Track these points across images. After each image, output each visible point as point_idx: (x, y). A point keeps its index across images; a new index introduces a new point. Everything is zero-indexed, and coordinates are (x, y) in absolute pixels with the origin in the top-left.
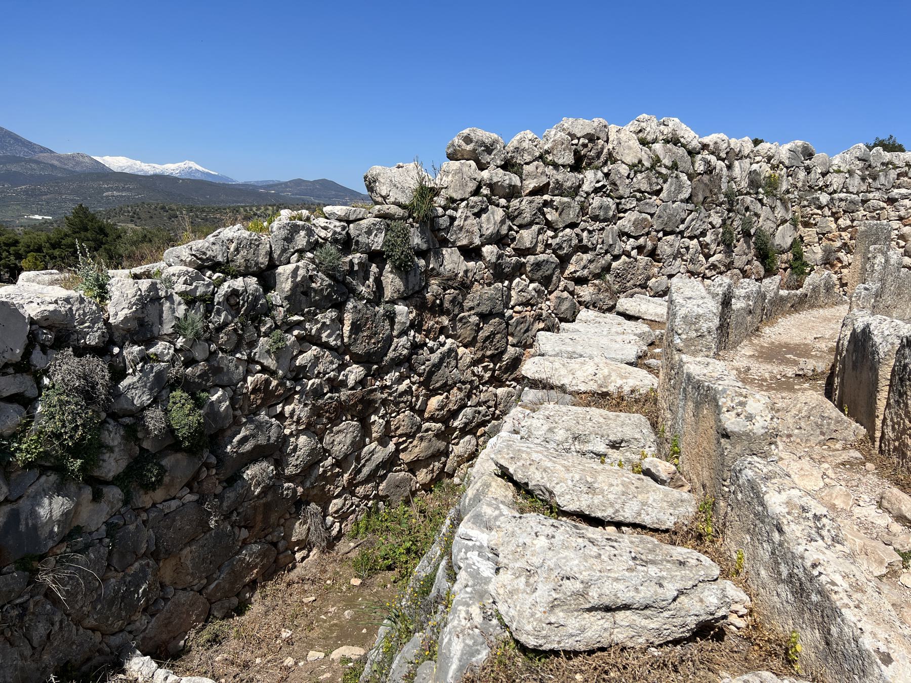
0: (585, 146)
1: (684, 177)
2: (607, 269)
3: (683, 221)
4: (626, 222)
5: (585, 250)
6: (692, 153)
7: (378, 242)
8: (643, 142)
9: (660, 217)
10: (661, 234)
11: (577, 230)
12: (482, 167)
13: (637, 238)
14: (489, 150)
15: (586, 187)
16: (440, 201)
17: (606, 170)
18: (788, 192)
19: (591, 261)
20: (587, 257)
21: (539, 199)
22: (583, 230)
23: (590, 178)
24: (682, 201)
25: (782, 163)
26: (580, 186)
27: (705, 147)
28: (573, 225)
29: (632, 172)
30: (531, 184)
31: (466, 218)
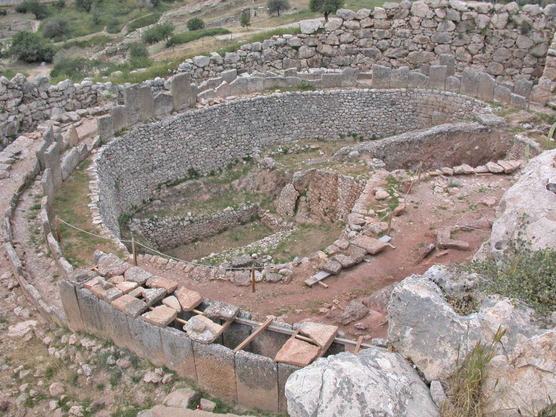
0: (393, 12)
1: (450, 23)
2: (406, 55)
3: (453, 39)
4: (416, 39)
5: (394, 48)
6: (461, 12)
7: (296, 44)
8: (431, 8)
9: (434, 37)
10: (436, 44)
11: (389, 40)
12: (344, 20)
13: (422, 44)
14: (347, 15)
17: (406, 19)
18: (545, 28)
19: (396, 52)
20: (393, 50)
22: (392, 40)
23: (396, 22)
24: (449, 32)
25: (543, 13)
26: (391, 25)
27: (471, 9)
28: (386, 39)
29: (421, 21)
30: (365, 25)
31: (333, 37)
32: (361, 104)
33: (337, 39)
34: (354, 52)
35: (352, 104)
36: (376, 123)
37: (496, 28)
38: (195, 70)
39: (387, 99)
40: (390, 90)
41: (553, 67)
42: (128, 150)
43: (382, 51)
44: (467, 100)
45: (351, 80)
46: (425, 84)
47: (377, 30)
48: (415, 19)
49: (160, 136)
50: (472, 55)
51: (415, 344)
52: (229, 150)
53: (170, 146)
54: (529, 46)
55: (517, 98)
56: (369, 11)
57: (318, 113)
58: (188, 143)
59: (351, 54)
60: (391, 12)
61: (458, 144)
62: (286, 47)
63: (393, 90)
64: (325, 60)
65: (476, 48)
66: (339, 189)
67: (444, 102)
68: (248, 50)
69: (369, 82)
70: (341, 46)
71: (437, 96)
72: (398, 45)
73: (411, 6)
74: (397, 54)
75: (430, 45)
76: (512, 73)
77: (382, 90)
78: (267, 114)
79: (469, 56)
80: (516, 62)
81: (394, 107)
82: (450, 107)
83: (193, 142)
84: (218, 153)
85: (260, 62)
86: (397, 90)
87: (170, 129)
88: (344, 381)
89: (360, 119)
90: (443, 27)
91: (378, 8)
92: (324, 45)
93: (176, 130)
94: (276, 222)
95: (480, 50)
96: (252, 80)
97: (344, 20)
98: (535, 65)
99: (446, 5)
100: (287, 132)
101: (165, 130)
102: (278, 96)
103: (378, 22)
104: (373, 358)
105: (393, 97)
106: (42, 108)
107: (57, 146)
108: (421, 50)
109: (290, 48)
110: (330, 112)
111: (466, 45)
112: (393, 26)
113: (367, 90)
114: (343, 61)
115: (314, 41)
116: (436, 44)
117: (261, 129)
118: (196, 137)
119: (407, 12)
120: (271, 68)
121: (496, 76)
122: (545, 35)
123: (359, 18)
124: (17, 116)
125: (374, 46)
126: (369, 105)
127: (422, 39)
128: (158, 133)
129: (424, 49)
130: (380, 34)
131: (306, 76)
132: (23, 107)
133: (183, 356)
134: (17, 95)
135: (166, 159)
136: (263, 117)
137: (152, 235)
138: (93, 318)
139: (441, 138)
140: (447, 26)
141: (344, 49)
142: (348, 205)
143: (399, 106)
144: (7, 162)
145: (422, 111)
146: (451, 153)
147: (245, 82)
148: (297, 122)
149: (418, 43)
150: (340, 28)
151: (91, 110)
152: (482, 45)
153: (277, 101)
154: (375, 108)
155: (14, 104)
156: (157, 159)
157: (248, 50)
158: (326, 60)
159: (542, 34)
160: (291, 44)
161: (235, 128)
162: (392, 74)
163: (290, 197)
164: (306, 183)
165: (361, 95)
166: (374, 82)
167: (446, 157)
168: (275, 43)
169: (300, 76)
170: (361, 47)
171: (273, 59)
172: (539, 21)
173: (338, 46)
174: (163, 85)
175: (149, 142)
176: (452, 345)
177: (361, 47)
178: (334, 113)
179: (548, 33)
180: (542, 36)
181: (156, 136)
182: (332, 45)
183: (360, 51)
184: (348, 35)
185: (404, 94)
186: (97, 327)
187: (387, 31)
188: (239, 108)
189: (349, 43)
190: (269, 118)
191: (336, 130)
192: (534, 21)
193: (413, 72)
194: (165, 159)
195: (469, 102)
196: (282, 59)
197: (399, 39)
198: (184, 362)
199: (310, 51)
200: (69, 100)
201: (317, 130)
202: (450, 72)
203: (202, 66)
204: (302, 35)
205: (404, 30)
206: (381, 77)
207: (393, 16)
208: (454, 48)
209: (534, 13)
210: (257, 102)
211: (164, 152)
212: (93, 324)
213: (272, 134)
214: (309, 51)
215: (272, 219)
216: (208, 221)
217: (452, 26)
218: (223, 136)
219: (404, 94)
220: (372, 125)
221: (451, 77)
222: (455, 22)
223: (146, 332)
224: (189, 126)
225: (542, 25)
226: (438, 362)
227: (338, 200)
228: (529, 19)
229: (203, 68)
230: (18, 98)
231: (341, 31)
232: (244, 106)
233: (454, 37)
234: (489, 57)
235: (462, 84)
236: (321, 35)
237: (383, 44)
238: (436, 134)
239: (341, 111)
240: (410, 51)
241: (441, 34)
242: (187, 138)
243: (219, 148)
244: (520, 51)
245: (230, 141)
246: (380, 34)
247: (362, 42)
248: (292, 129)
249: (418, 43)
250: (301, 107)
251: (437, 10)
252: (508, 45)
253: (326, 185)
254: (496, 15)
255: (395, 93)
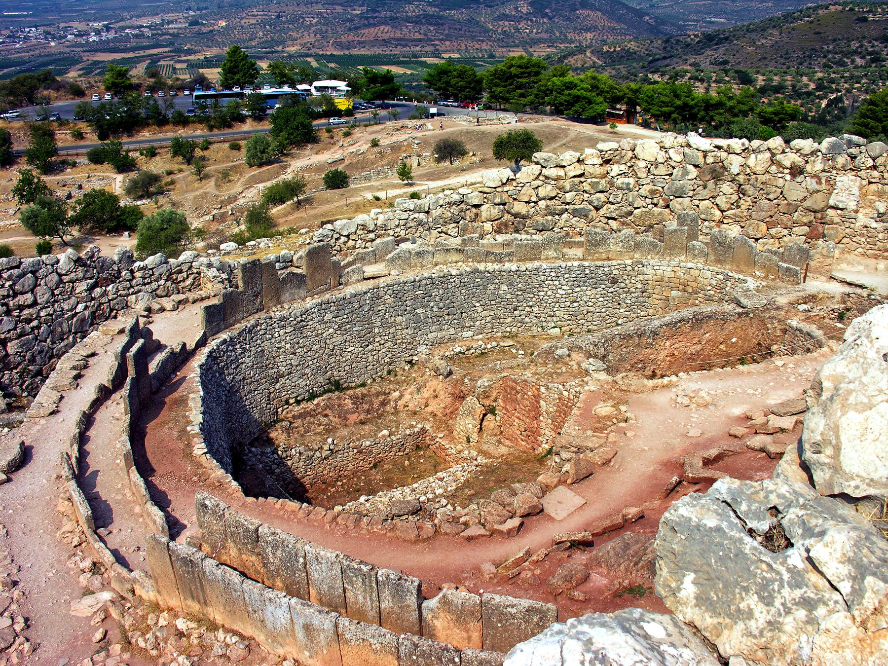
2: (631, 213)
4: (643, 192)
5: (613, 204)
6: (705, 154)
7: (476, 202)
10: (672, 197)
15: (613, 174)
16: (515, 184)
17: (629, 164)
18: (824, 171)
20: (613, 207)
21: (577, 180)
23: (615, 169)
27: (719, 148)
29: (649, 166)
32: (570, 284)
33: (533, 193)
34: (557, 212)
35: (557, 283)
36: (591, 309)
37: (754, 174)
38: (337, 239)
39: (606, 275)
40: (610, 263)
41: (836, 224)
42: (244, 350)
43: (597, 209)
44: (717, 273)
45: (555, 250)
46: (658, 253)
47: (589, 180)
48: (642, 164)
49: (289, 330)
50: (722, 211)
51: (701, 600)
52: (384, 350)
53: (301, 345)
54: (801, 197)
55: (787, 269)
56: (578, 154)
57: (509, 296)
58: (328, 341)
59: (553, 215)
60: (607, 155)
61: (707, 335)
62: (462, 206)
63: (614, 263)
64: (519, 223)
65: (727, 202)
66: (542, 403)
67: (686, 278)
68: (410, 211)
69: (579, 252)
70: (540, 203)
71: (676, 269)
72: (619, 200)
73: (635, 146)
74: (617, 212)
75: (663, 200)
76: (779, 236)
77: (599, 263)
78: (437, 299)
79: (718, 213)
80: (785, 218)
81: (615, 286)
82: (694, 284)
83: (334, 340)
84: (369, 354)
85: (427, 227)
86: (619, 262)
87: (302, 321)
88: (596, 658)
89: (568, 304)
90: (680, 173)
91: (588, 151)
92: (515, 202)
93: (310, 323)
94: (453, 451)
95: (732, 204)
96: (418, 253)
97: (542, 167)
98: (810, 222)
99: (683, 144)
100: (467, 325)
101: (295, 322)
102: (454, 273)
103: (590, 169)
104: (637, 622)
105: (615, 272)
106: (123, 293)
107: (144, 345)
108: (650, 206)
109: (468, 207)
110: (526, 295)
111: (713, 197)
112: (612, 174)
113: (576, 264)
114: (542, 224)
115: (501, 197)
116: (672, 197)
117: (430, 321)
118: (339, 332)
119: (630, 154)
120: (442, 235)
121: (757, 240)
122: (823, 181)
123: (564, 164)
124: (88, 304)
125: (584, 203)
126: (581, 284)
127: (653, 192)
128: (284, 327)
129: (656, 205)
130: (593, 185)
131: (493, 246)
132: (98, 291)
133: (323, 643)
134: (88, 275)
135: (296, 363)
136: (432, 304)
137: (277, 471)
138: (193, 588)
139: (683, 328)
140: (686, 173)
141: (544, 207)
142: (555, 425)
143: (623, 285)
144: (74, 368)
145: (656, 291)
146: (698, 347)
147: (407, 255)
148: (480, 309)
149: (646, 197)
150: (537, 178)
151: (191, 296)
152: (735, 197)
153: (452, 280)
154: (589, 288)
155: (85, 288)
156: (284, 364)
157: (410, 211)
158: (519, 222)
159: (820, 179)
160: (469, 201)
161: (393, 319)
162: (613, 241)
163: (473, 416)
164: (494, 394)
165: (569, 270)
166: (587, 251)
167: (692, 354)
168: (447, 200)
169: (483, 246)
170: (568, 204)
171: (446, 223)
172: (814, 161)
173: (536, 203)
174: (291, 261)
175: (273, 340)
176: (761, 598)
177: (568, 204)
178: (532, 296)
179: (828, 177)
180: (819, 183)
181: (282, 332)
182: (527, 202)
183: (567, 210)
184: (549, 187)
185: (629, 268)
186: (199, 602)
187: (603, 181)
188: (400, 291)
189: (551, 199)
190: (441, 305)
191: (535, 320)
192: (807, 162)
193: (640, 238)
194: (294, 362)
195: (721, 277)
196: (458, 223)
197: (620, 192)
198: (325, 652)
199: (496, 211)
200: (162, 282)
201: (509, 320)
202: (693, 236)
203: (345, 233)
204: (486, 190)
205: (626, 180)
206: (597, 244)
207: (610, 160)
208: (697, 202)
209: (807, 151)
210: (424, 282)
211: (294, 353)
212: (193, 599)
213: (446, 327)
214: (495, 211)
215: (447, 446)
216: (355, 451)
217: (693, 172)
218: (376, 330)
219: (629, 268)
220: (585, 312)
221: (694, 242)
222: (696, 166)
223: (270, 608)
224: (328, 316)
225: (819, 166)
226: (740, 626)
227: (541, 418)
228: (800, 159)
229: (348, 236)
230: (91, 278)
231: (540, 183)
232: (406, 288)
233: (696, 186)
234: (745, 214)
235: (710, 251)
236: (512, 188)
237: (598, 199)
238: (676, 323)
239: (541, 293)
240: (636, 208)
241: (678, 184)
242: (328, 333)
243: (370, 347)
244: (788, 205)
245: (386, 337)
246: (593, 185)
247: (569, 197)
248: (474, 320)
249: (646, 197)
250: (485, 288)
251: (671, 152)
252: (771, 197)
253: (523, 398)
254: (753, 156)
255: (617, 267)
